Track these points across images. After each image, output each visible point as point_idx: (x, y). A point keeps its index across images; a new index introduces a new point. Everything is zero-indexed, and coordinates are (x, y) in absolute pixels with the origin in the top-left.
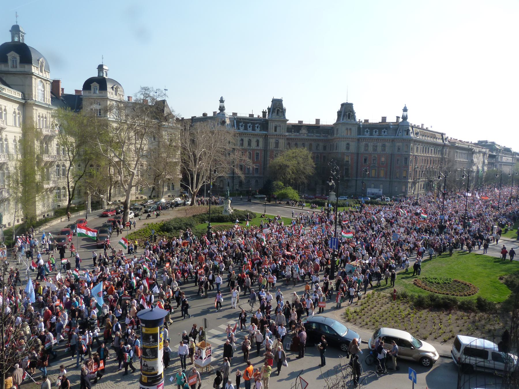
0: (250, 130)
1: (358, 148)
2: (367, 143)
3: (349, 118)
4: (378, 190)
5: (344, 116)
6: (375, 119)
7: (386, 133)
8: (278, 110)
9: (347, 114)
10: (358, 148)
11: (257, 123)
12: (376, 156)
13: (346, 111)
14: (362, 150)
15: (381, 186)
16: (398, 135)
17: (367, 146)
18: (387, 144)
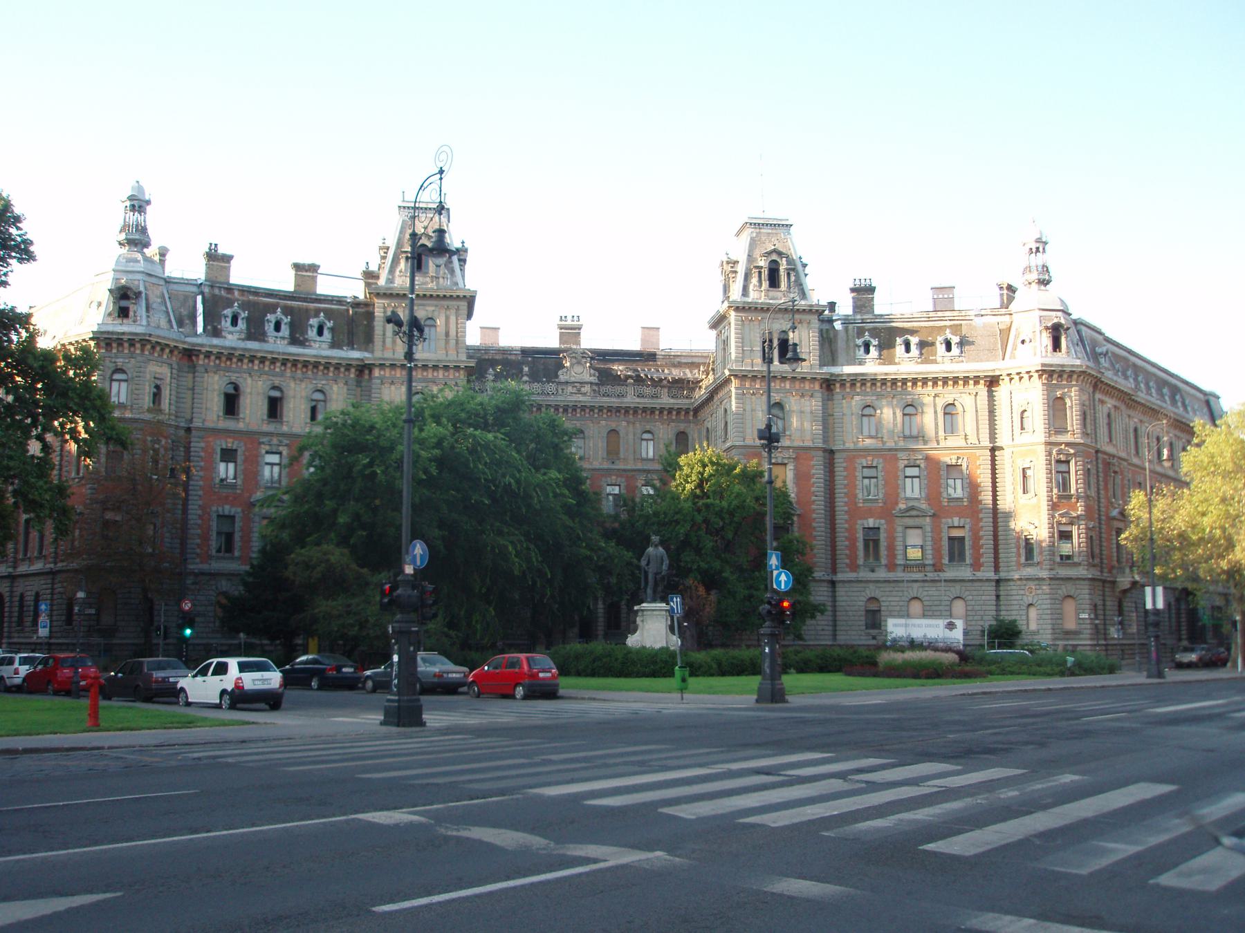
0: (277, 344)
4: (942, 623)
11: (317, 313)
15: (959, 607)
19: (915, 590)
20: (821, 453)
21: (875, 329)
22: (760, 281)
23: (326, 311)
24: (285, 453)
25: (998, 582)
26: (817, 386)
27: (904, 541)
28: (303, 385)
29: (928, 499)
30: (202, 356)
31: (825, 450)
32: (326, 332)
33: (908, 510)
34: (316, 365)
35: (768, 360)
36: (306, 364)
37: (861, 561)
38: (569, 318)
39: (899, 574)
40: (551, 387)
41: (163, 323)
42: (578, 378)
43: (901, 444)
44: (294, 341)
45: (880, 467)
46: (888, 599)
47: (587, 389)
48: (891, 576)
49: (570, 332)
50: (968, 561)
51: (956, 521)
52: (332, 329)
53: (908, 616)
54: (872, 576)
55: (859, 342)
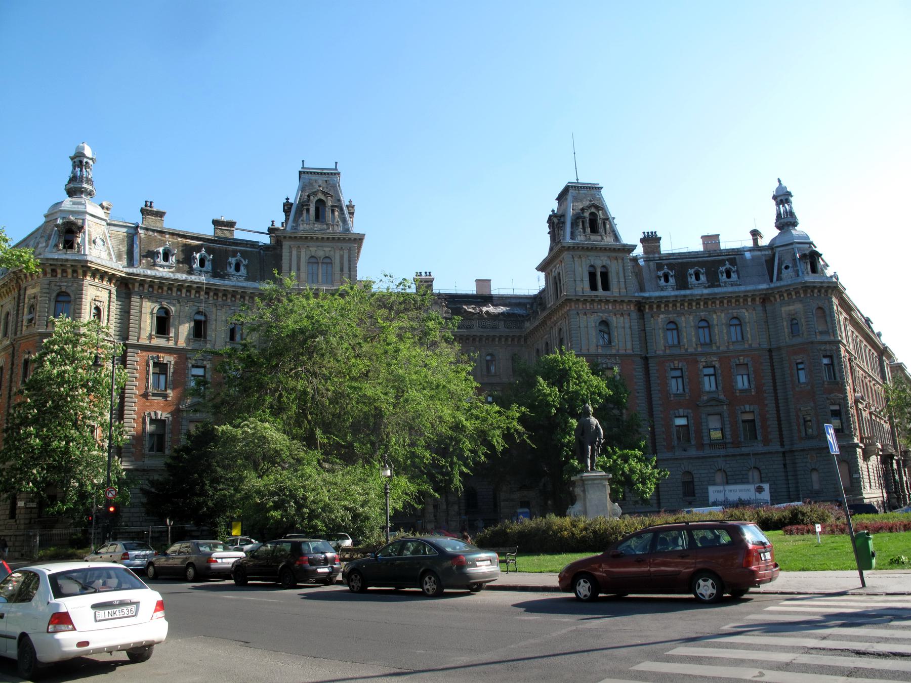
1: (644, 336)
2: (673, 316)
3: (594, 229)
4: (752, 487)
5: (574, 224)
6: (680, 241)
7: (734, 276)
8: (320, 202)
9: (587, 214)
10: (644, 336)
11: (234, 254)
12: (715, 360)
13: (580, 218)
14: (661, 342)
16: (779, 278)
17: (673, 325)
18: (746, 314)
21: (670, 264)
22: (584, 228)
23: (242, 253)
24: (208, 366)
25: (784, 453)
27: (707, 425)
28: (223, 311)
30: (137, 285)
32: (242, 268)
33: (708, 401)
34: (234, 294)
35: (593, 287)
36: (225, 293)
37: (675, 442)
38: (423, 274)
39: (707, 452)
41: (104, 255)
44: (215, 274)
48: (700, 453)
49: (425, 282)
50: (759, 438)
51: (747, 408)
52: (246, 266)
55: (661, 273)
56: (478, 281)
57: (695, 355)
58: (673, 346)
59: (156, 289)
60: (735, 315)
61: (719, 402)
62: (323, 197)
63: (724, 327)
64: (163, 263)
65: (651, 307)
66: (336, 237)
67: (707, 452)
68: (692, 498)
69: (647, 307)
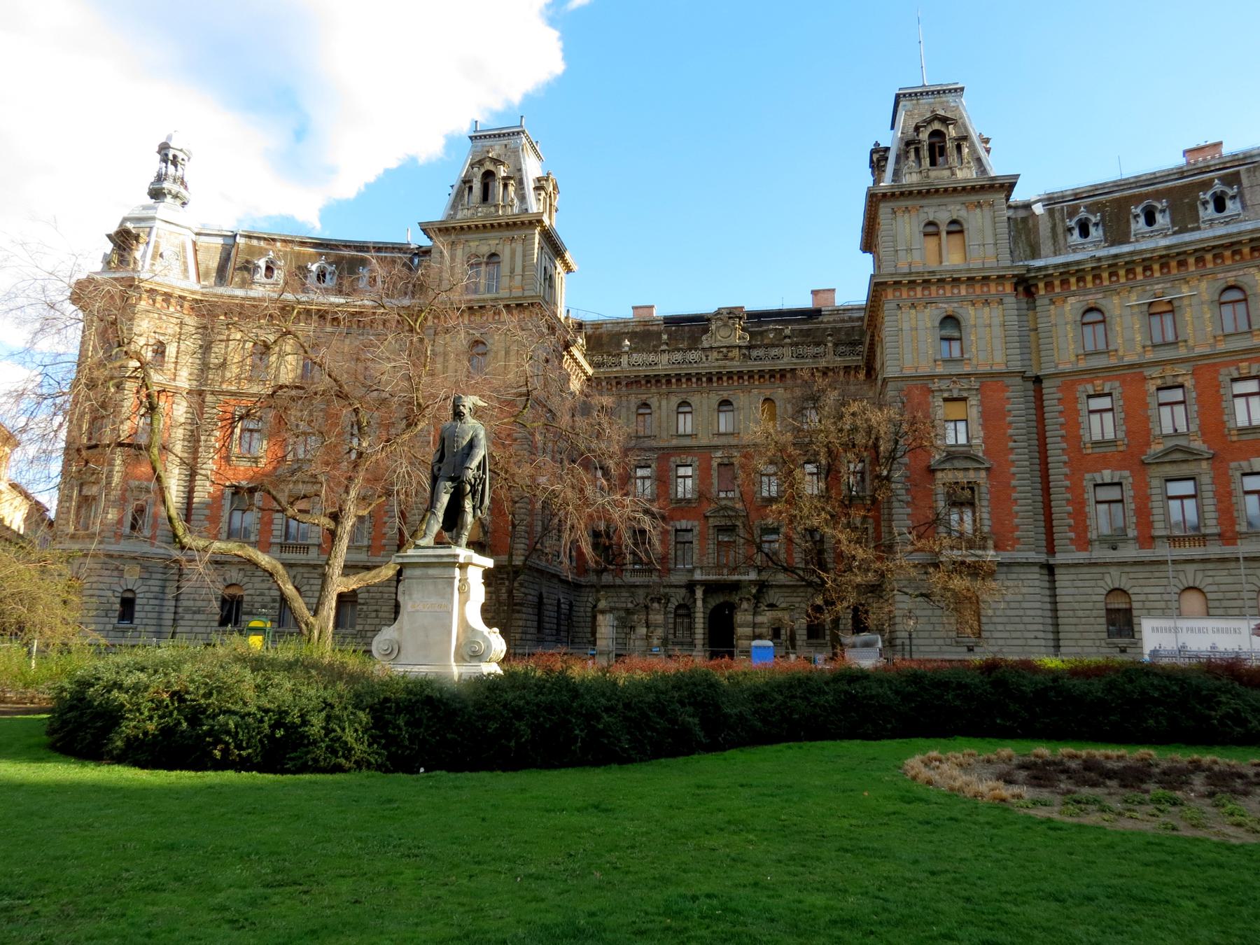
1: (1031, 338)
9: (924, 136)
10: (1031, 338)
19: (1190, 575)
20: (1018, 380)
21: (1096, 203)
26: (1009, 288)
29: (1204, 432)
31: (1022, 375)
33: (1167, 452)
39: (1163, 551)
40: (693, 355)
42: (726, 342)
43: (1150, 356)
45: (1116, 394)
46: (1140, 588)
47: (736, 352)
48: (1146, 554)
53: (1180, 615)
54: (1110, 555)
56: (815, 293)
57: (1140, 365)
58: (1097, 353)
59: (243, 312)
60: (1231, 281)
61: (1191, 455)
62: (492, 168)
63: (1205, 308)
64: (264, 280)
65: (1049, 285)
66: (503, 222)
67: (1163, 551)
68: (1127, 640)
69: (1041, 285)
